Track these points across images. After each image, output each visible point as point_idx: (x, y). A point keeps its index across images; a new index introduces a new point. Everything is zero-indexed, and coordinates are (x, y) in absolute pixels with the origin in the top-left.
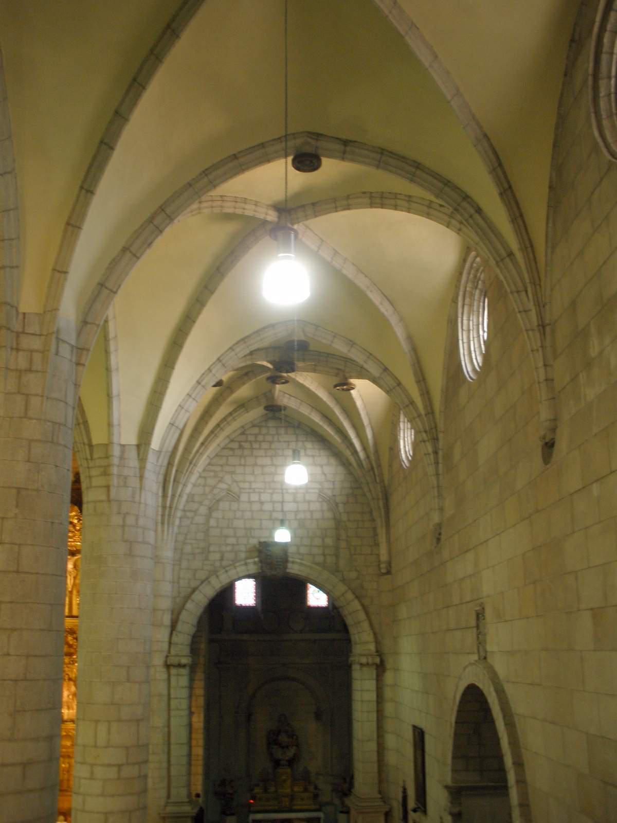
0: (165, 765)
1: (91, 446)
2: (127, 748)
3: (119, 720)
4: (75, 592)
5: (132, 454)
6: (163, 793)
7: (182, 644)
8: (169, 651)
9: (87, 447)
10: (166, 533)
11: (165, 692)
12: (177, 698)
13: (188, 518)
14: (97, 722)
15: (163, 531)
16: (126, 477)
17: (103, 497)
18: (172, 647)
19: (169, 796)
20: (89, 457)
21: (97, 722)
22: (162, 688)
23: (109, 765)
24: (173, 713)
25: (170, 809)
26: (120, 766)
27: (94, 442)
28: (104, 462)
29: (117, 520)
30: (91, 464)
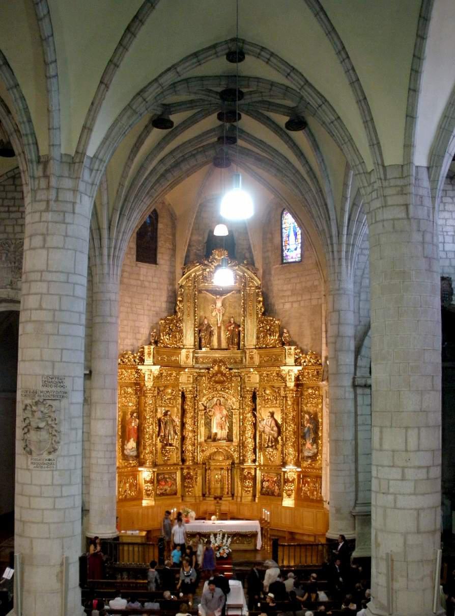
0: (353, 472)
1: (384, 166)
2: (433, 450)
3: (428, 426)
4: (223, 328)
5: (424, 175)
6: (352, 496)
7: (365, 367)
8: (355, 374)
9: (381, 167)
10: (349, 268)
11: (353, 409)
12: (362, 415)
13: (365, 255)
14: (407, 428)
16: (421, 197)
17: (403, 215)
18: (358, 370)
19: (356, 499)
20: (382, 177)
21: (407, 428)
22: (350, 405)
23: (419, 467)
24: (359, 428)
25: (358, 509)
26: (428, 467)
27: (386, 164)
28: (400, 182)
29: (417, 237)
30: (386, 184)
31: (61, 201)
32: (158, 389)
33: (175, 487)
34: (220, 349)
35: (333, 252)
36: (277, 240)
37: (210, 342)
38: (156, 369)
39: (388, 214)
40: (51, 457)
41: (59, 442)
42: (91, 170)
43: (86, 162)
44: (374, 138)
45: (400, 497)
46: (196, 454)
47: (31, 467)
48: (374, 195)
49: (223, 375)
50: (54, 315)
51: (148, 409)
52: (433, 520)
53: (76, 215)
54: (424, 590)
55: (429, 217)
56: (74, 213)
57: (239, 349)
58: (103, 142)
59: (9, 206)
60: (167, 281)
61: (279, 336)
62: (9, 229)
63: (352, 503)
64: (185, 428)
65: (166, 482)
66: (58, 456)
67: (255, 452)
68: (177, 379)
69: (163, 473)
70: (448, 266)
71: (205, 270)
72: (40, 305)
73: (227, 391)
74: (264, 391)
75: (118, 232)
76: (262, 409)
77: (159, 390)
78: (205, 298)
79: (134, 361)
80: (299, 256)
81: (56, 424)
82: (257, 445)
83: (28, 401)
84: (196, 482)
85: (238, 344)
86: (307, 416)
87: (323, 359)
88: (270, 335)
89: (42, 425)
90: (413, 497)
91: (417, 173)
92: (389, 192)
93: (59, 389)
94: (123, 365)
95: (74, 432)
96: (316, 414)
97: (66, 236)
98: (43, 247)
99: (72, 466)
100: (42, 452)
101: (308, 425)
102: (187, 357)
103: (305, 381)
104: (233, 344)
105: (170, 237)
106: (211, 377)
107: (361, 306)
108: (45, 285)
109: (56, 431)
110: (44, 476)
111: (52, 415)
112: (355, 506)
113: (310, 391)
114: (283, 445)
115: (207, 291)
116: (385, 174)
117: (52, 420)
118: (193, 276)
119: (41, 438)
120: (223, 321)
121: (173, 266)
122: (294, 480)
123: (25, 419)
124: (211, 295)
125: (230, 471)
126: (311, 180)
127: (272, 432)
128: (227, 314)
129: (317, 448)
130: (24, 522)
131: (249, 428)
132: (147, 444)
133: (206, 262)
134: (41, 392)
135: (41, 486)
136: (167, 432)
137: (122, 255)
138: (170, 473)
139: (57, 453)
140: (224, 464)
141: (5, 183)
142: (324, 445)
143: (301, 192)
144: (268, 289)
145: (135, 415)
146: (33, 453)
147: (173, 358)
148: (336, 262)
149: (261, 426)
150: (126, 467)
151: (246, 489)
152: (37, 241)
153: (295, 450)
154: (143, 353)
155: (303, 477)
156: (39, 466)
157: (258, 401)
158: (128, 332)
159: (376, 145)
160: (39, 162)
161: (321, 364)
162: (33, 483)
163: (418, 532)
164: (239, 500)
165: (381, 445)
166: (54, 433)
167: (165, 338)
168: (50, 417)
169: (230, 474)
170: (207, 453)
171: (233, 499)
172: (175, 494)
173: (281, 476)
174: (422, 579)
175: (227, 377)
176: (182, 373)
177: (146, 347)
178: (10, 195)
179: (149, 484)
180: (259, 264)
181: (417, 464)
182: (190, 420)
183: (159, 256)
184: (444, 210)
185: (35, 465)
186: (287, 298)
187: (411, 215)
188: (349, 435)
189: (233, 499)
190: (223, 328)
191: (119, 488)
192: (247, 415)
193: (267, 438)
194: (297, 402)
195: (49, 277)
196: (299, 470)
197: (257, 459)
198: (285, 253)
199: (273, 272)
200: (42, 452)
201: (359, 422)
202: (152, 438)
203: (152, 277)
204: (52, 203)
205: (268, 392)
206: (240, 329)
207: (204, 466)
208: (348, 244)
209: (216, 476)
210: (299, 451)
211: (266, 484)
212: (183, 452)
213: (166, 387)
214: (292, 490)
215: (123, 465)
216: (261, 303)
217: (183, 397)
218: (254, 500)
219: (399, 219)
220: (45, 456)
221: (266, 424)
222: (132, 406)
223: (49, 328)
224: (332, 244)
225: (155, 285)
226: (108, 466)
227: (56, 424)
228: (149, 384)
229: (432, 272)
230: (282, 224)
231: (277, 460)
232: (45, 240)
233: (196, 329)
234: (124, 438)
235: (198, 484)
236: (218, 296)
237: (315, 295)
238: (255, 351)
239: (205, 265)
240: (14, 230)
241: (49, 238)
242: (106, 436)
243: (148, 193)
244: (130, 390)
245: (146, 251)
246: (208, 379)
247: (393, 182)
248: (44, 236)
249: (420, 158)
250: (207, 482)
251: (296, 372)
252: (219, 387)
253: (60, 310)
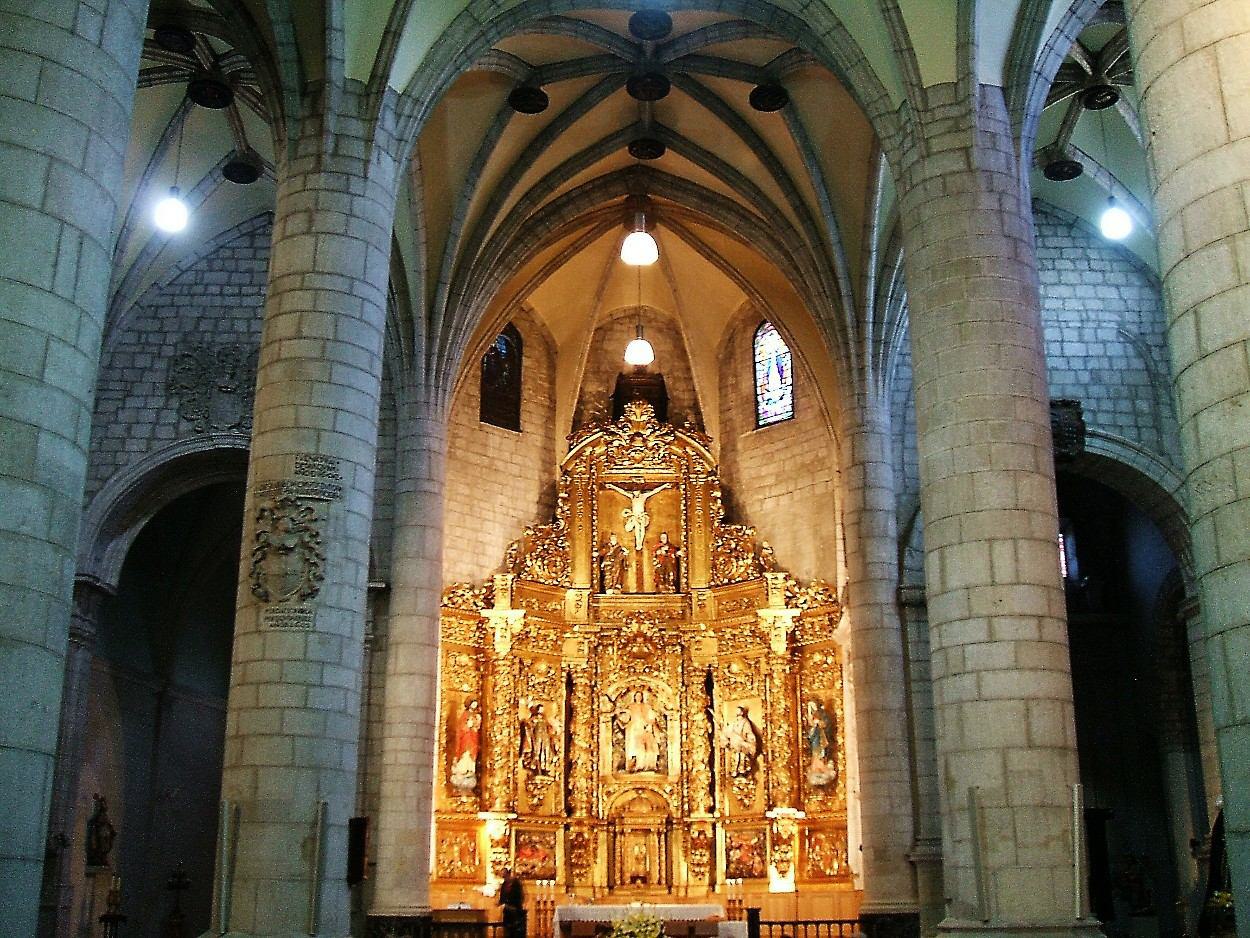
0: (906, 776)
1: (924, 91)
3: (1031, 538)
5: (996, 100)
10: (880, 384)
14: (991, 540)
15: (877, 381)
16: (994, 135)
17: (962, 166)
19: (916, 831)
21: (991, 540)
22: (894, 642)
23: (1022, 616)
24: (914, 687)
26: (1040, 617)
28: (955, 111)
31: (344, 156)
32: (521, 662)
33: (552, 862)
34: (640, 592)
35: (848, 357)
36: (746, 386)
37: (621, 580)
38: (516, 618)
39: (931, 169)
40: (306, 605)
41: (322, 579)
42: (398, 116)
43: (388, 99)
44: (902, 39)
45: (988, 677)
46: (594, 800)
47: (265, 626)
48: (908, 144)
49: (648, 640)
50: (324, 347)
51: (499, 696)
52: (1057, 724)
53: (369, 183)
54: (1053, 868)
55: (1009, 169)
56: (366, 177)
57: (678, 591)
58: (422, 69)
59: (240, 286)
60: (539, 465)
61: (753, 558)
62: (241, 326)
63: (908, 840)
64: (574, 745)
65: (534, 850)
66: (319, 605)
67: (712, 792)
68: (557, 647)
69: (529, 832)
70: (1074, 385)
71: (611, 443)
72: (299, 331)
73: (656, 673)
74: (729, 667)
75: (447, 326)
76: (726, 704)
77: (522, 668)
78: (612, 499)
79: (475, 603)
80: (790, 408)
81: (318, 543)
82: (717, 777)
83: (268, 504)
84: (595, 856)
85: (677, 583)
86: (812, 706)
87: (840, 591)
88: (737, 558)
89: (291, 542)
90: (1015, 675)
91: (983, 96)
92: (935, 129)
93: (327, 480)
94: (453, 610)
95: (351, 565)
96: (831, 703)
97: (351, 215)
98: (308, 232)
99: (346, 630)
101: (817, 721)
102: (578, 606)
103: (808, 640)
104: (666, 581)
105: (546, 385)
106: (625, 645)
107: (906, 459)
108: (308, 295)
109: (317, 555)
110: (291, 642)
111: (313, 526)
112: (914, 845)
113: (818, 657)
114: (769, 769)
115: (616, 485)
116: (925, 100)
117: (312, 536)
118: (588, 453)
120: (646, 542)
121: (550, 438)
122: (791, 837)
123: (258, 536)
124: (622, 491)
125: (663, 836)
126: (803, 222)
127: (744, 744)
128: (652, 528)
129: (836, 768)
130: (241, 737)
131: (699, 741)
132: (497, 766)
133: (613, 428)
135: (281, 661)
136: (537, 748)
137: (455, 371)
138: (543, 833)
139: (317, 599)
140: (651, 820)
141: (235, 244)
142: (849, 762)
143: (786, 254)
144: (731, 480)
145: (474, 705)
147: (551, 606)
148: (855, 373)
149: (723, 737)
150: (454, 812)
151: (697, 869)
152: (298, 223)
153: (791, 777)
154: (490, 589)
155: (811, 830)
156: (281, 623)
157: (716, 690)
158: (463, 550)
159: (903, 51)
160: (304, 94)
161: (835, 601)
162: (267, 656)
163: (1031, 746)
164: (682, 893)
165: (943, 582)
166: (314, 559)
167: (535, 567)
168: (307, 529)
169: (663, 843)
170: (618, 803)
171: (670, 893)
172: (553, 877)
173: (764, 834)
174: (1046, 845)
175: (654, 645)
176: (568, 635)
177: (498, 577)
178: (244, 265)
179: (501, 850)
180: (713, 430)
181: (1017, 610)
182: (584, 727)
183: (524, 417)
184: (1059, 283)
186: (767, 489)
187: (976, 162)
188: (894, 699)
189: (670, 893)
190: (646, 553)
191: (438, 853)
192: (696, 718)
193: (737, 760)
194: (793, 686)
195: (317, 281)
196: (801, 815)
197: (718, 806)
198: (762, 407)
199: (740, 446)
201: (914, 675)
202: (509, 753)
203: (512, 454)
204: (326, 159)
205: (735, 668)
206: (679, 553)
207: (611, 828)
208: (876, 342)
209: (634, 848)
210: (797, 772)
211: (735, 855)
212: (568, 793)
213: (535, 660)
214: (788, 861)
215: (449, 808)
216: (719, 501)
217: (570, 685)
218: (714, 890)
219: (953, 173)
220: (293, 603)
221: (733, 731)
222: (468, 687)
223: (314, 370)
224: (846, 344)
225: (515, 470)
226: (420, 766)
227: (318, 543)
228: (502, 647)
229: (1021, 263)
230: (754, 355)
231: (759, 804)
232: (311, 221)
233: (595, 554)
234: (452, 750)
235: (598, 860)
236: (636, 493)
237: (822, 477)
238: (709, 592)
239: (613, 434)
240: (249, 326)
241: (318, 217)
242: (416, 708)
243: (501, 261)
244: (464, 659)
245: (501, 406)
246: (619, 649)
247: (939, 114)
248: (311, 214)
249: (988, 70)
250: (618, 858)
251: (790, 625)
252: (640, 666)
253: (336, 340)
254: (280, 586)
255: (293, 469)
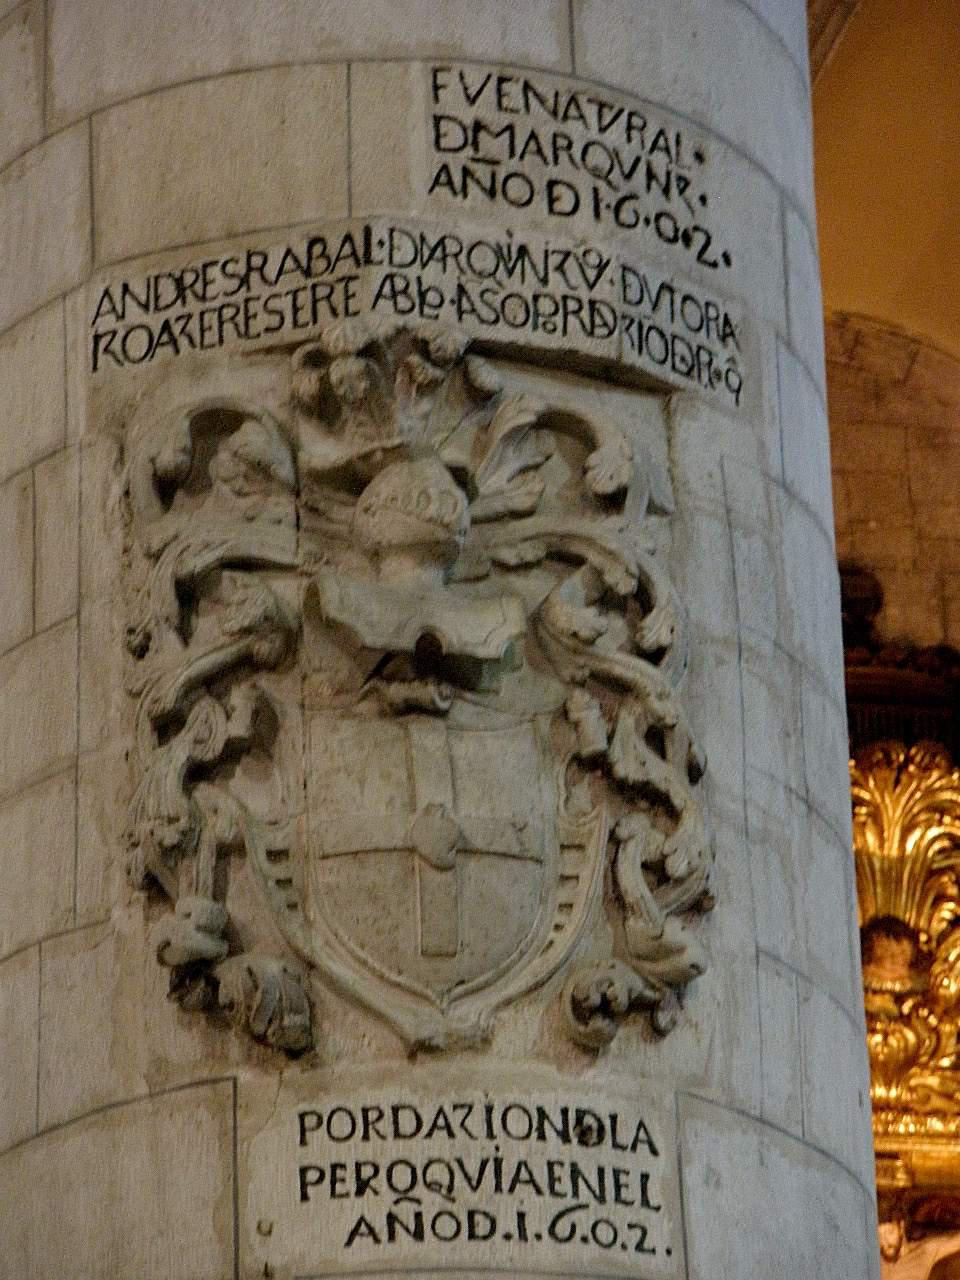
40: (599, 1087)
66: (691, 1092)
89: (481, 627)
100: (470, 1013)
119: (474, 815)
123: (190, 593)
134: (436, 251)
139: (681, 1048)
146: (339, 1034)
166: (632, 761)
168: (563, 557)
185: (375, 1207)
200: (470, 1013)
227: (655, 656)
254: (411, 937)
255: (422, 161)
